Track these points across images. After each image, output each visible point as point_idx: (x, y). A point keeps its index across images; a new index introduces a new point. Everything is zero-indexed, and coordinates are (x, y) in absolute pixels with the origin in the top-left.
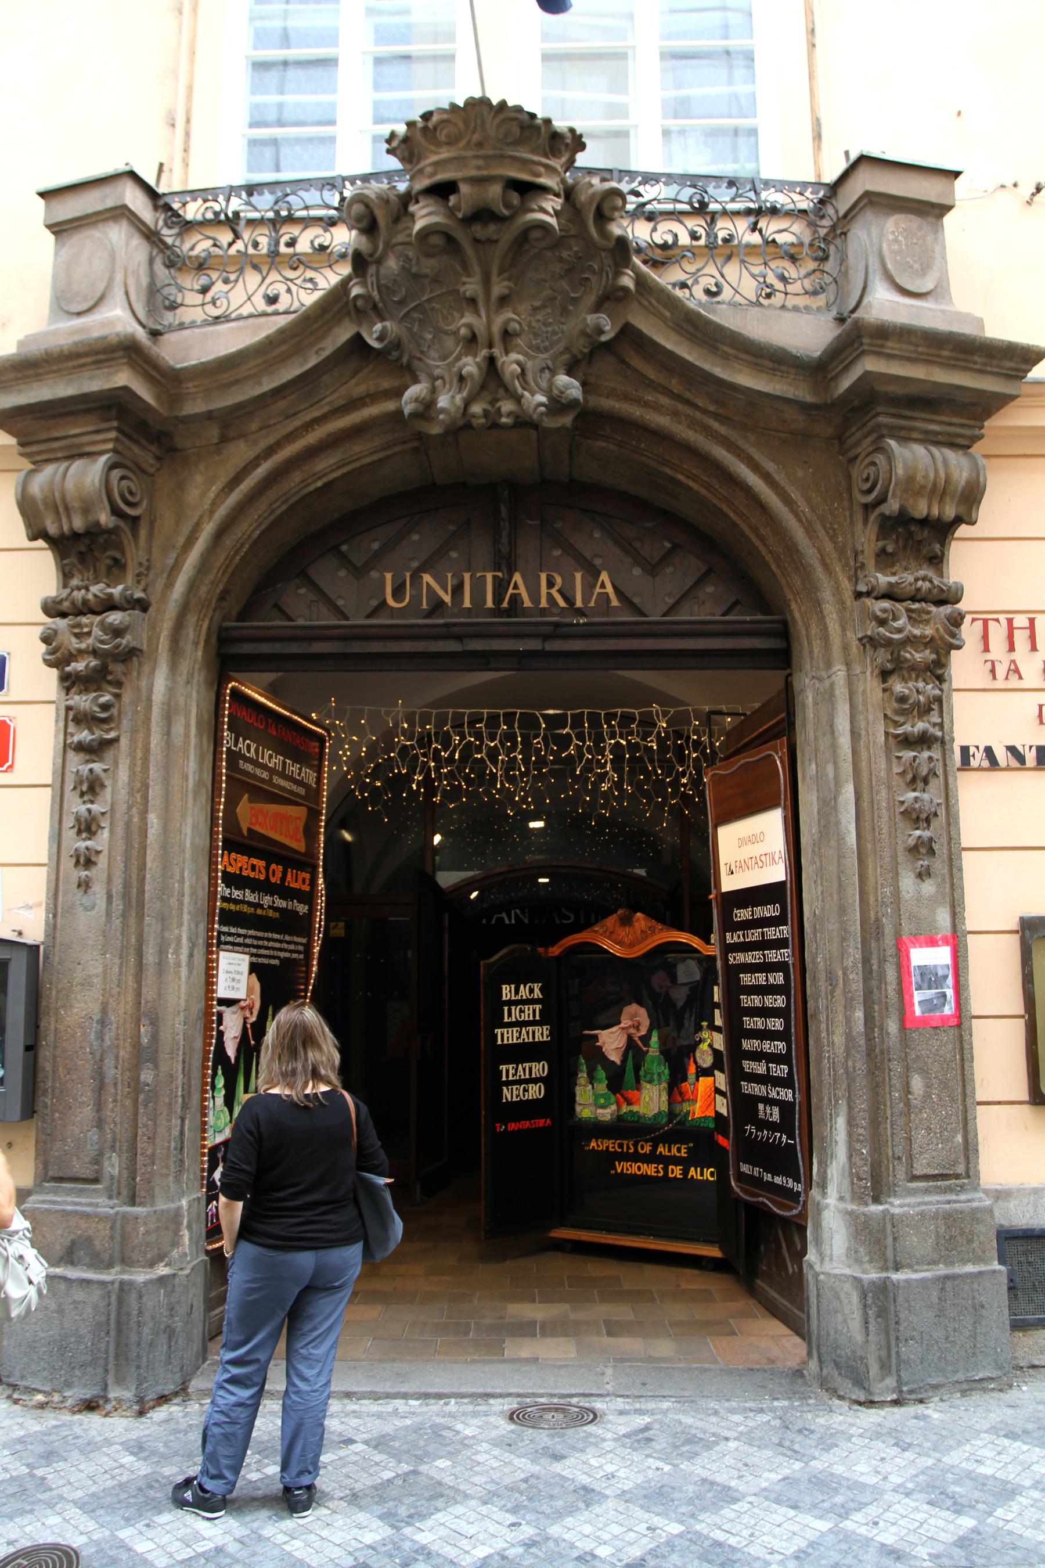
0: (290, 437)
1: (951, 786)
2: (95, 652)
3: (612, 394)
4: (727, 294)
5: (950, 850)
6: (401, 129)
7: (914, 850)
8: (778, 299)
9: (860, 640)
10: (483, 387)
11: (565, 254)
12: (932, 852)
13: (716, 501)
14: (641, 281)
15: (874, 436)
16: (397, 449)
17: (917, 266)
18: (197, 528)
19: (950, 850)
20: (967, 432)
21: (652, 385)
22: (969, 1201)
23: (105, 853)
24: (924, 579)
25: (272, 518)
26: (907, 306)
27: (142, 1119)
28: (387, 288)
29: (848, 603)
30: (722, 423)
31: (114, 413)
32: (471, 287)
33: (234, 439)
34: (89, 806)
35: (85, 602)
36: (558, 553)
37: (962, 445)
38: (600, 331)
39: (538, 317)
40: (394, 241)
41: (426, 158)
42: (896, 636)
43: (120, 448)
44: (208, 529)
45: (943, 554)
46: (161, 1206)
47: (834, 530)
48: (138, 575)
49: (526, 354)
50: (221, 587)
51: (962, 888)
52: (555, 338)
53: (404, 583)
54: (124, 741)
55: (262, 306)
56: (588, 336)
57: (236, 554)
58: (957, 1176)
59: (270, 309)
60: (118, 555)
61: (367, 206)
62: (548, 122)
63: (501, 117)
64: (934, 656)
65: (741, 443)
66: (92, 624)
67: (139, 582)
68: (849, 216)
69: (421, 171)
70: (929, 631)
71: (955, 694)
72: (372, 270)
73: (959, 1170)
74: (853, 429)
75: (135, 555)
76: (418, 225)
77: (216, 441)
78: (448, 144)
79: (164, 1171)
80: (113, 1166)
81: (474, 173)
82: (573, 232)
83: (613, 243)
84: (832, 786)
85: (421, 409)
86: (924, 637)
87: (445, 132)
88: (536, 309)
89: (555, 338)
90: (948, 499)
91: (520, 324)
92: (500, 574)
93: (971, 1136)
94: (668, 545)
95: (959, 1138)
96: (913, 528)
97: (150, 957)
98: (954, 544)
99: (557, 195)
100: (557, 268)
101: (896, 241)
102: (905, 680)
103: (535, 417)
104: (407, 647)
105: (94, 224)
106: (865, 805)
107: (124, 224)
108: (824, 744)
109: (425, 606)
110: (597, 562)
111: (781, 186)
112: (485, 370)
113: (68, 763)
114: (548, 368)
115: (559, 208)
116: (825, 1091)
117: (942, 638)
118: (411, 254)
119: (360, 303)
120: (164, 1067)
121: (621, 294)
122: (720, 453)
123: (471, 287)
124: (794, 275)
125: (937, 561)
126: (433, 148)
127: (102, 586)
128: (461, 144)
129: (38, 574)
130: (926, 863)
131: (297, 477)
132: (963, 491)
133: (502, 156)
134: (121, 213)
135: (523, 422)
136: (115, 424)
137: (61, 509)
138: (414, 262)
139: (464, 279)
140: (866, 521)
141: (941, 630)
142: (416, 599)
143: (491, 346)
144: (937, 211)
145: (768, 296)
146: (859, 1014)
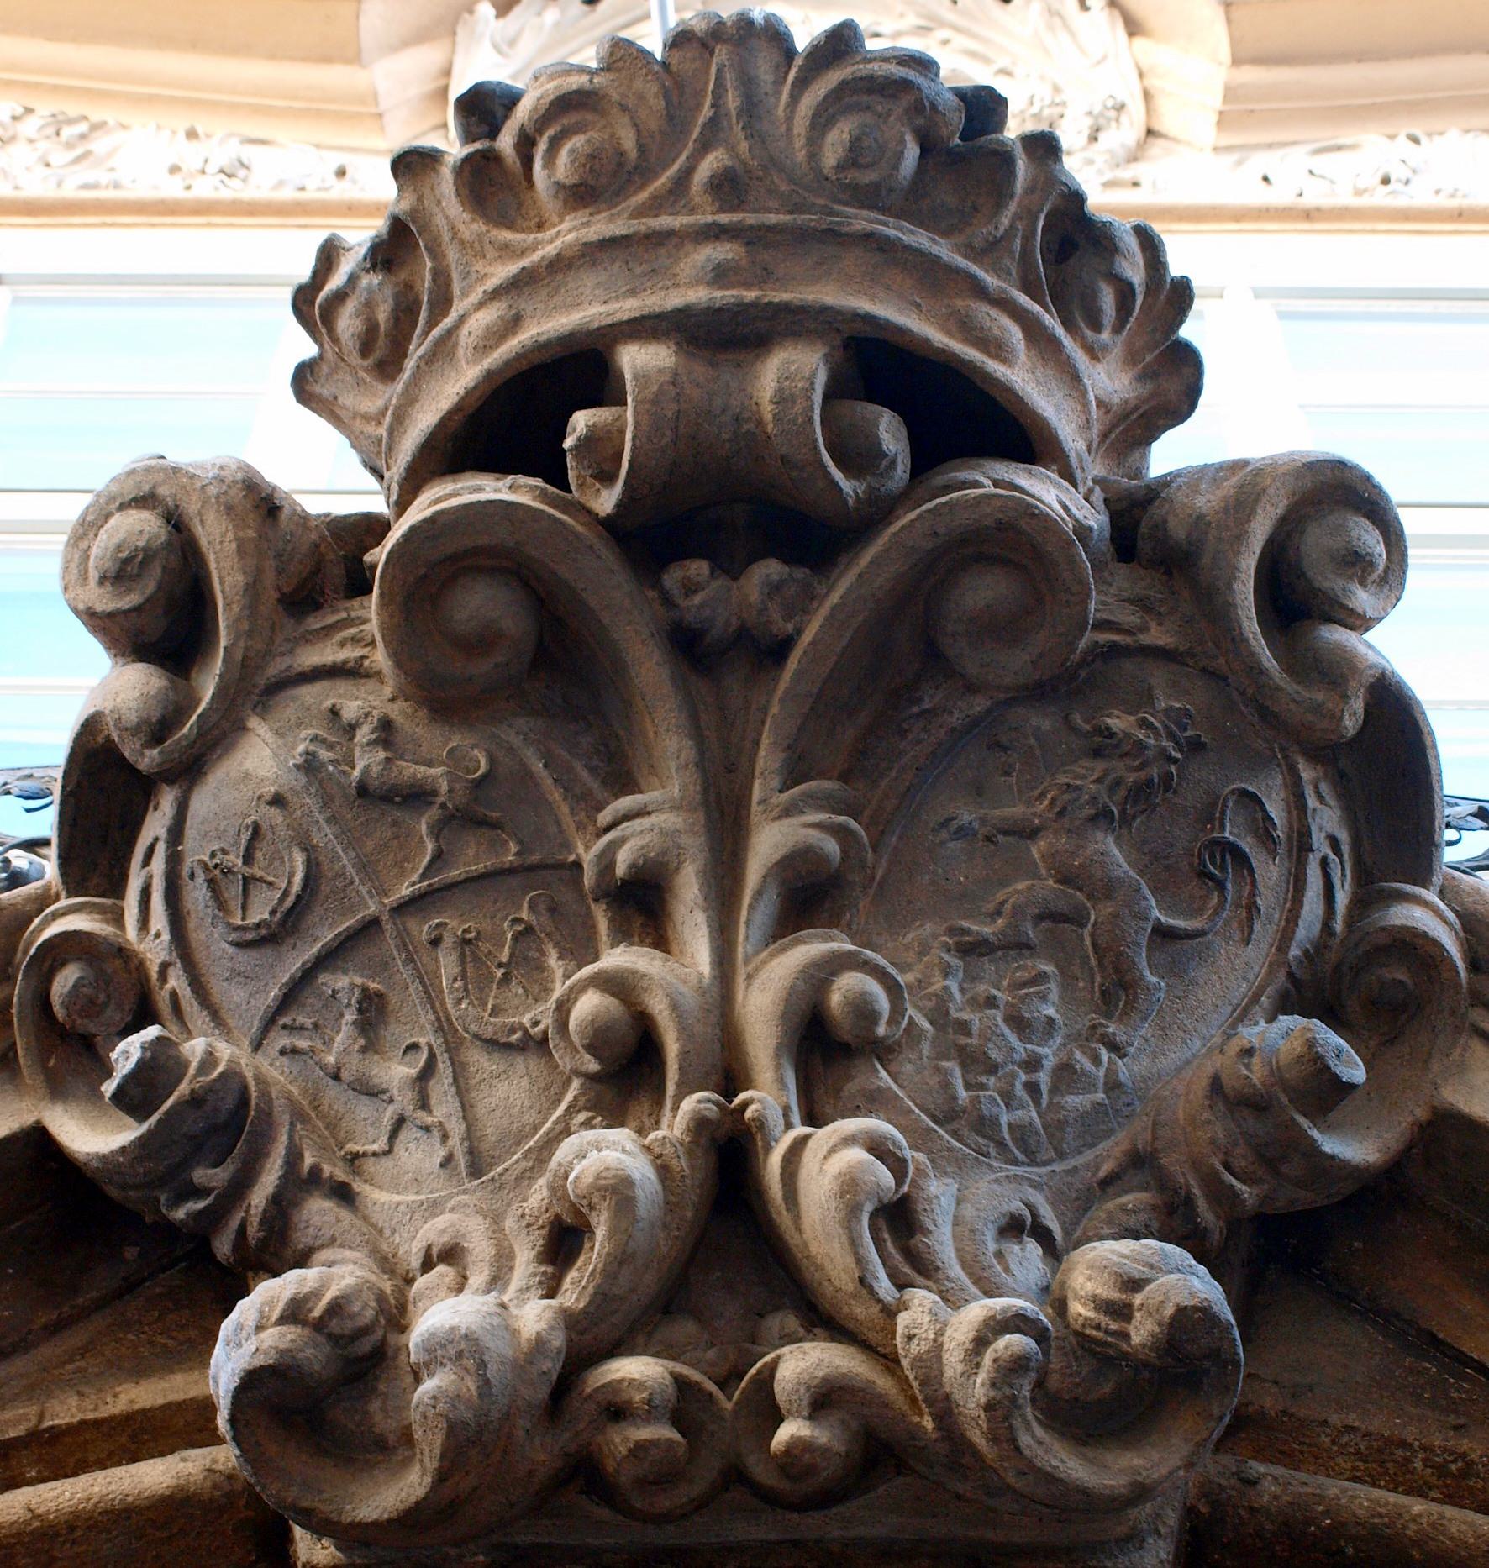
52: (1076, 1101)
62: (1044, 146)
81: (699, 295)
82: (1157, 636)
85: (316, 1357)
88: (972, 949)
112: (692, 1197)
114: (1042, 1235)
118: (351, 709)
133: (833, 236)
138: (364, 734)
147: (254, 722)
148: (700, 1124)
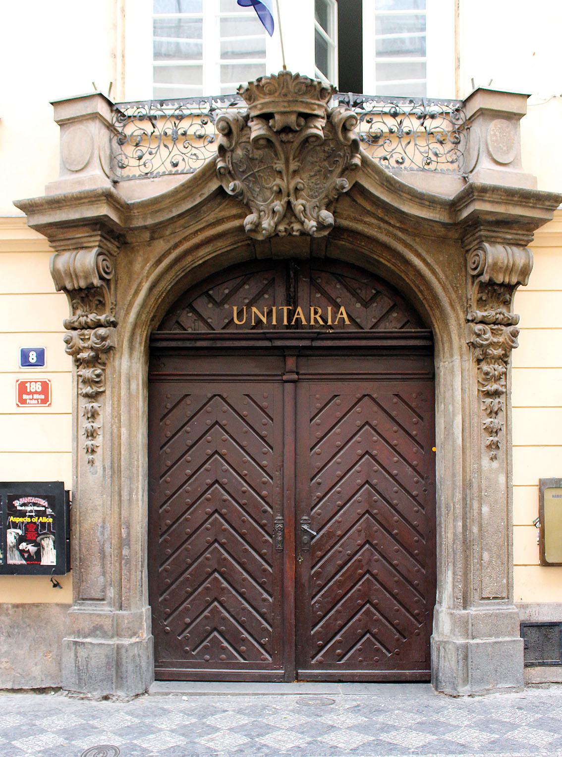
0: (186, 239)
1: (509, 416)
2: (92, 348)
3: (348, 218)
4: (407, 163)
5: (507, 447)
6: (245, 85)
7: (489, 447)
8: (432, 166)
9: (468, 344)
10: (285, 216)
11: (326, 148)
12: (498, 447)
13: (398, 272)
14: (364, 160)
15: (478, 240)
16: (239, 244)
17: (505, 148)
18: (140, 285)
19: (507, 447)
20: (526, 238)
21: (368, 213)
22: (508, 609)
23: (101, 446)
24: (500, 314)
25: (177, 279)
26: (497, 171)
27: (124, 572)
28: (236, 164)
29: (462, 325)
30: (403, 233)
31: (98, 227)
32: (279, 165)
33: (157, 239)
34: (92, 424)
35: (86, 323)
36: (318, 295)
37: (522, 244)
38: (343, 188)
39: (313, 181)
40: (241, 141)
41: (258, 100)
42: (485, 343)
43: (101, 245)
44: (146, 286)
45: (510, 300)
46: (134, 611)
47: (457, 287)
48: (111, 309)
49: (306, 200)
50: (152, 314)
51: (512, 465)
52: (321, 191)
53: (243, 310)
54: (108, 393)
55: (170, 168)
56: (337, 190)
57: (159, 298)
58: (503, 598)
59: (174, 170)
60: (101, 299)
61: (228, 123)
63: (296, 81)
64: (503, 352)
65: (414, 245)
66: (90, 334)
67: (112, 312)
68: (471, 119)
69: (255, 107)
70: (501, 339)
71: (513, 369)
72: (229, 154)
73: (504, 595)
74: (468, 236)
75: (109, 299)
76: (253, 135)
77: (149, 239)
78: (270, 94)
79: (135, 595)
80: (111, 593)
81: (283, 109)
82: (331, 137)
83: (351, 142)
84: (451, 415)
85: (254, 228)
86: (499, 342)
87: (268, 88)
88: (311, 176)
89: (321, 191)
90: (513, 274)
91: (303, 185)
92: (291, 308)
93: (510, 580)
94: (374, 292)
95: (505, 581)
96: (496, 288)
97: (125, 497)
98: (517, 293)
99: (323, 118)
100: (322, 155)
101: (495, 135)
102: (488, 363)
103: (311, 233)
104: (244, 344)
105: (81, 121)
106: (467, 425)
107: (97, 121)
108: (448, 394)
109: (253, 324)
110: (339, 300)
111: (437, 102)
112: (285, 208)
113: (80, 403)
114: (317, 206)
115: (324, 125)
116: (443, 559)
117: (507, 343)
119: (222, 171)
120: (133, 547)
121: (354, 167)
122: (400, 248)
123: (279, 165)
124: (442, 152)
125: (507, 303)
126: (261, 95)
127: (94, 315)
128: (276, 94)
129: (60, 308)
130: (494, 453)
131: (189, 259)
132: (521, 270)
134: (95, 116)
135: (304, 233)
136: (99, 232)
137: (74, 277)
138: (250, 152)
139: (276, 161)
140: (473, 283)
141: (507, 339)
142: (249, 319)
143: (288, 195)
144: (517, 117)
145: (428, 164)
146: (460, 524)
147: (238, 147)
148: (286, 202)
